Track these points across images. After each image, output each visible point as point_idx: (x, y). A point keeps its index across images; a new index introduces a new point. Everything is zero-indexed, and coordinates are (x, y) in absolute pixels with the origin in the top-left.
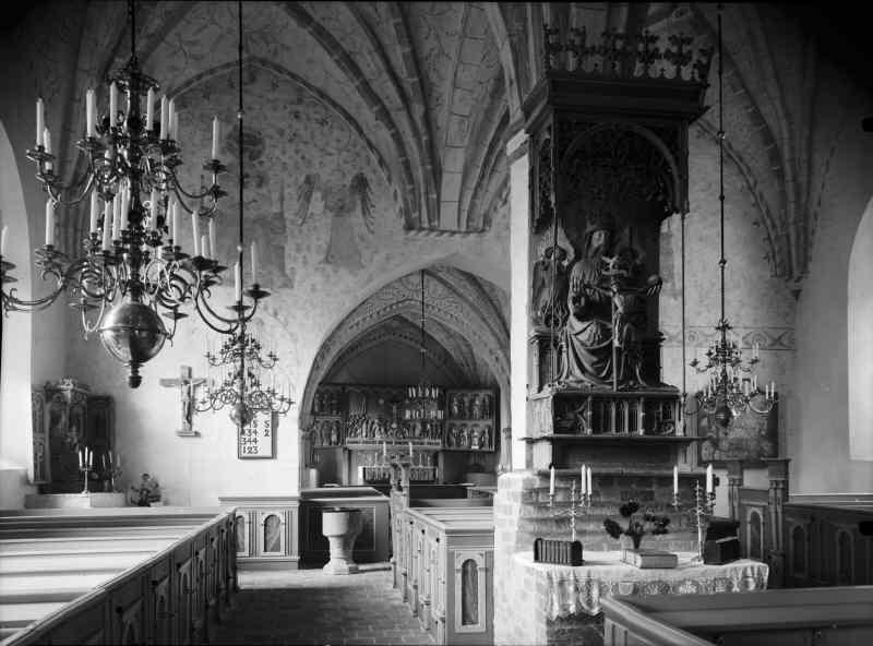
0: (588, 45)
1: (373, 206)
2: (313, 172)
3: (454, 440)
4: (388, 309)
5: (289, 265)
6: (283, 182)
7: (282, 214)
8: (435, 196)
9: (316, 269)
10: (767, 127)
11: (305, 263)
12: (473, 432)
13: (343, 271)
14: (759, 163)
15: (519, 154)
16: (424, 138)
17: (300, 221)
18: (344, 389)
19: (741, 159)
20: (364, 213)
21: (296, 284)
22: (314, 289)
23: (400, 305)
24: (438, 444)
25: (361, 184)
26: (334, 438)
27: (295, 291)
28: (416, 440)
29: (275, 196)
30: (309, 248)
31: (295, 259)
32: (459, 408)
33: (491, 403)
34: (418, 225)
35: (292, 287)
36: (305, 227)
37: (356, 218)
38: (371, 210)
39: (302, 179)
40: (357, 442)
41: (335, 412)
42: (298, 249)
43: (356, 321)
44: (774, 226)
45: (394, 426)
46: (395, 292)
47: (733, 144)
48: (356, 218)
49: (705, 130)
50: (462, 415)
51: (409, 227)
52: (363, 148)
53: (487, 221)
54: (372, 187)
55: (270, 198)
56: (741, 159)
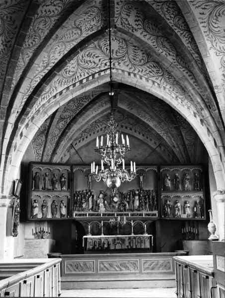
4: (91, 78)
12: (185, 203)
18: (72, 169)
23: (102, 73)
24: (155, 215)
26: (64, 211)
28: (135, 212)
43: (59, 90)
45: (116, 199)
46: (97, 60)
50: (176, 189)
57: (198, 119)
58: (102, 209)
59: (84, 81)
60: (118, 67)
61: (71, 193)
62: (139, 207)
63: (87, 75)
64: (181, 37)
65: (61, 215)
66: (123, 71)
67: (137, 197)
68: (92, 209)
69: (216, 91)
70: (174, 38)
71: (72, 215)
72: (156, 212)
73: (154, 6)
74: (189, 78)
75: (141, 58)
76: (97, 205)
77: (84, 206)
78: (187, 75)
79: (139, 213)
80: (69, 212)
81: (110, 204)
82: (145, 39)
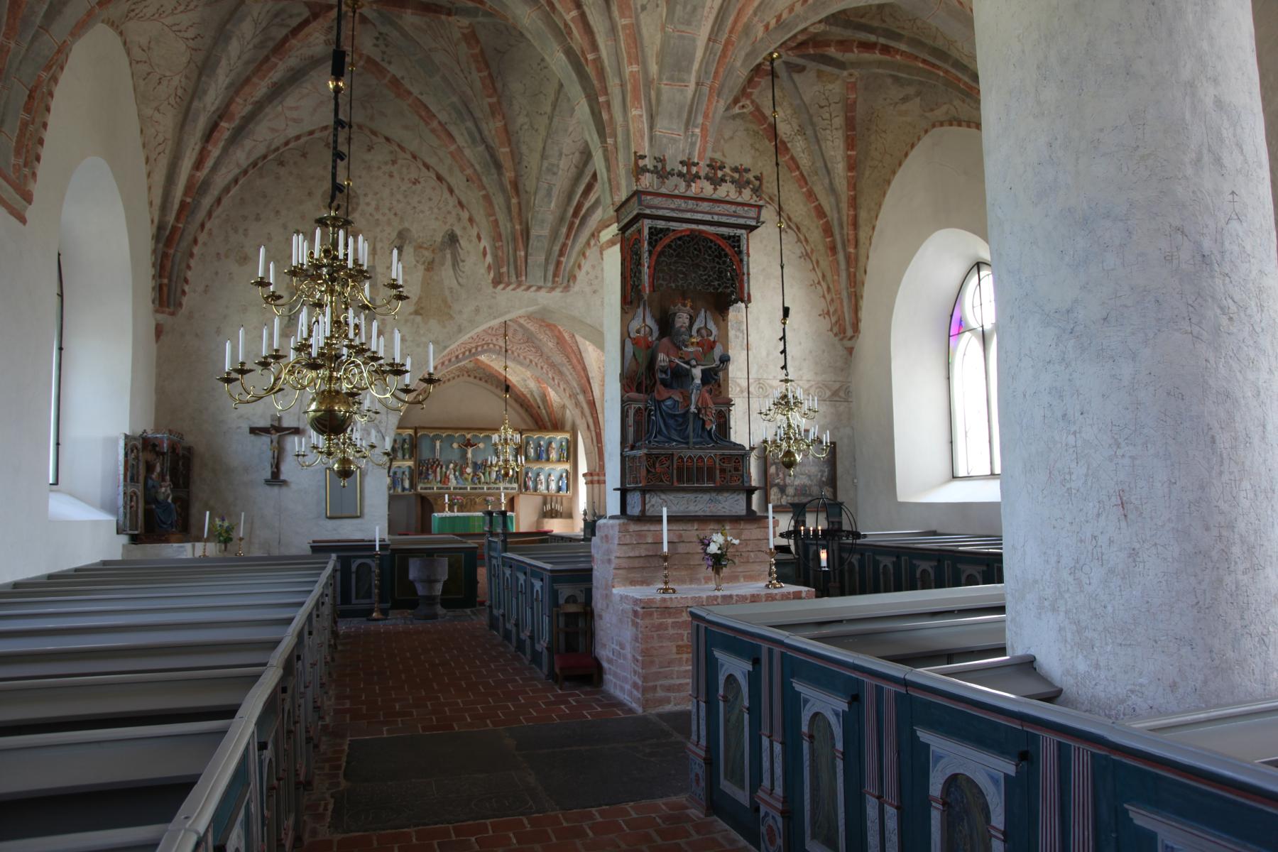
0: (668, 169)
2: (406, 225)
3: (530, 484)
8: (523, 253)
9: (406, 321)
13: (433, 323)
14: (815, 235)
15: (612, 243)
16: (514, 201)
18: (416, 433)
19: (798, 229)
20: (454, 265)
25: (452, 239)
26: (407, 484)
32: (536, 450)
33: (568, 448)
34: (506, 279)
39: (394, 235)
44: (829, 289)
45: (469, 470)
48: (446, 272)
50: (538, 458)
51: (496, 282)
53: (572, 277)
56: (798, 229)
65: (404, 489)
72: (516, 485)
76: (446, 477)
80: (413, 486)
81: (462, 473)
82: (529, 326)
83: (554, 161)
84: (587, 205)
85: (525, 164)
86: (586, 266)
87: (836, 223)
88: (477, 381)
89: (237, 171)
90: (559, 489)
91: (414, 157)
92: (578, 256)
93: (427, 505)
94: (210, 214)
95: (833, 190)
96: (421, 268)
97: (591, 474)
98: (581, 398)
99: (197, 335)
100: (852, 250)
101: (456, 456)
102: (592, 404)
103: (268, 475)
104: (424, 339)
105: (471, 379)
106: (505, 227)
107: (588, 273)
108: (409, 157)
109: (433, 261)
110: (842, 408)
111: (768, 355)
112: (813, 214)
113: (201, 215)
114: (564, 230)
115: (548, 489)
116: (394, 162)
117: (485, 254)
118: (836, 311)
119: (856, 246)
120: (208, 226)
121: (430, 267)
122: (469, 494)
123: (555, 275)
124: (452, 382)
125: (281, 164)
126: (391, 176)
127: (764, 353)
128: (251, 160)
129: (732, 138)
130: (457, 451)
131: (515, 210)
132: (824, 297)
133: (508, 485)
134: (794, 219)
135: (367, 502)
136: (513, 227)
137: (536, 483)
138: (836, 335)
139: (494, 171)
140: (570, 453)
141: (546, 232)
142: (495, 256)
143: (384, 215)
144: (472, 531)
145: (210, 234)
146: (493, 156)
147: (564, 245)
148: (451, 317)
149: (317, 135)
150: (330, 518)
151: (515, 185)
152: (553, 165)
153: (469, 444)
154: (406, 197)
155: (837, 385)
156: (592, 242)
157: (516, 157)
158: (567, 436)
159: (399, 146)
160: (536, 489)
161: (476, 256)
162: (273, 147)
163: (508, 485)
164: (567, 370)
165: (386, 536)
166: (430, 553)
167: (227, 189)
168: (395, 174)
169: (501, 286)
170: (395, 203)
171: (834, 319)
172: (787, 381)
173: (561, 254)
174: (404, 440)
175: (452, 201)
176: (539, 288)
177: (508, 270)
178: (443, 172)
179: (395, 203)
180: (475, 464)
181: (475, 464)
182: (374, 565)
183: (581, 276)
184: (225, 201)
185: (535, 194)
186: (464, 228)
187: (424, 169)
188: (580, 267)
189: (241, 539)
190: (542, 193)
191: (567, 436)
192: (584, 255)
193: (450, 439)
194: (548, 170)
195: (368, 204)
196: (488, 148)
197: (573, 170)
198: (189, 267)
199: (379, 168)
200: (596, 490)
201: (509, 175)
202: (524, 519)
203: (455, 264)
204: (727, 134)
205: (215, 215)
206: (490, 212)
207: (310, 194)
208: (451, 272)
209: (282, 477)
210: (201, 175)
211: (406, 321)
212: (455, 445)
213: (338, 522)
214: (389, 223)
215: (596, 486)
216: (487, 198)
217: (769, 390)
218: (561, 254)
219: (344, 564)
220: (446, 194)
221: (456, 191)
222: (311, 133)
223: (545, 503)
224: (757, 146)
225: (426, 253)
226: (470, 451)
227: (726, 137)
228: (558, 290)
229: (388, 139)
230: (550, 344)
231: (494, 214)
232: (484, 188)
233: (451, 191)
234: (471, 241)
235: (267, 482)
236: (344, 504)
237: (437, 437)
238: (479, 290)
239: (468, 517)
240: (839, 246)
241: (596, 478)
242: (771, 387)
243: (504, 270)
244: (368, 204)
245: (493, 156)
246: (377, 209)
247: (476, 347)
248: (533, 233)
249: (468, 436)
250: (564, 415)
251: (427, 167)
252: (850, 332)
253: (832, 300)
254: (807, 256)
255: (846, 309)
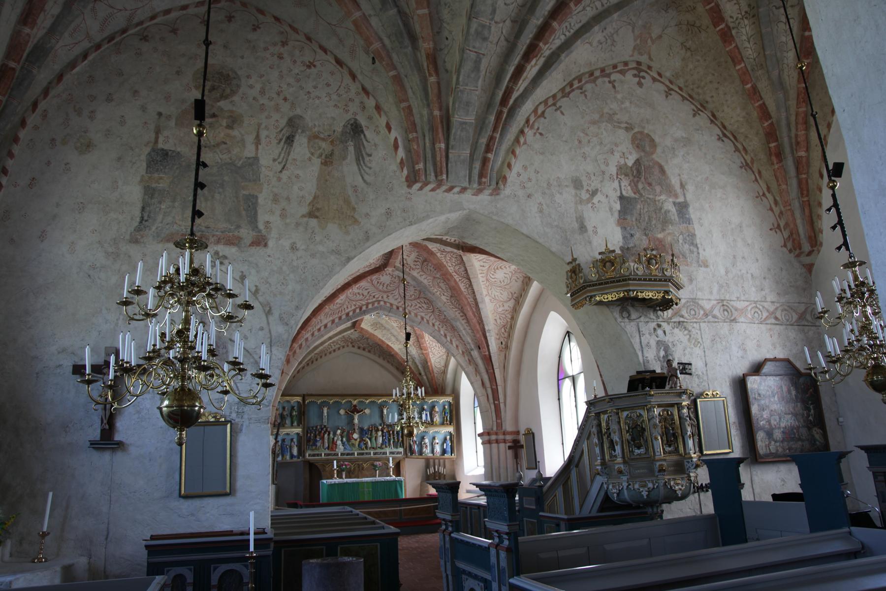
1: (370, 155)
2: (298, 111)
3: (416, 448)
4: (358, 311)
5: (262, 218)
6: (259, 125)
7: (256, 159)
8: (443, 146)
9: (298, 225)
10: (764, 103)
11: (283, 216)
12: (434, 438)
13: (333, 228)
14: (755, 142)
16: (433, 79)
17: (280, 167)
18: (304, 400)
19: (735, 137)
20: (358, 160)
21: (271, 243)
22: (293, 248)
25: (355, 130)
26: (295, 451)
27: (268, 251)
28: (379, 451)
29: (250, 139)
30: (288, 199)
31: (272, 212)
35: (266, 245)
36: (285, 175)
37: (348, 168)
38: (367, 159)
39: (283, 122)
40: (318, 455)
41: (295, 424)
42: (276, 199)
45: (356, 436)
46: (365, 293)
47: (726, 124)
48: (348, 168)
49: (699, 110)
51: (411, 181)
52: (358, 94)
53: (502, 179)
54: (366, 133)
55: (243, 140)
57: (467, 358)
58: (340, 448)
59: (351, 314)
60: (386, 300)
61: (303, 429)
62: (382, 444)
63: (353, 307)
64: (460, 283)
65: (292, 456)
66: (391, 305)
67: (380, 433)
68: (328, 448)
69: (487, 334)
70: (453, 283)
71: (304, 456)
72: (401, 450)
73: (438, 255)
74: (461, 319)
75: (412, 293)
77: (319, 444)
78: (459, 316)
79: (382, 451)
80: (301, 452)
82: (422, 279)
83: (485, 20)
84: (515, 95)
85: (446, 33)
86: (517, 167)
87: (784, 123)
88: (359, 351)
89: (86, 45)
90: (444, 452)
91: (309, 39)
92: (507, 152)
93: (315, 471)
94: (46, 93)
95: (780, 85)
96: (317, 162)
97: (489, 434)
98: (475, 353)
99: (12, 241)
100: (802, 153)
101: (342, 422)
102: (488, 360)
103: (95, 433)
104: (321, 248)
105: (355, 350)
106: (421, 113)
107: (519, 175)
108: (303, 39)
109: (332, 154)
110: (811, 333)
111: (727, 272)
112: (755, 114)
113: (35, 91)
114: (492, 118)
115: (433, 451)
116: (284, 44)
117: (396, 147)
118: (787, 225)
119: (807, 150)
120: (42, 105)
121: (328, 161)
122: (357, 460)
123: (481, 175)
124: (338, 353)
125: (145, 39)
126: (280, 57)
127: (723, 272)
128: (106, 34)
129: (660, 37)
130: (343, 417)
131: (432, 92)
132: (771, 209)
133: (394, 450)
134: (729, 127)
135: (241, 472)
136: (431, 114)
137: (421, 446)
138: (790, 251)
139: (407, 42)
140: (453, 416)
141: (471, 119)
142: (408, 151)
143: (271, 99)
144: (361, 499)
145: (45, 115)
146: (406, 25)
147: (491, 138)
148: (356, 221)
149: (191, 10)
150: (186, 497)
151: (433, 59)
152: (483, 26)
153: (355, 410)
154: (298, 81)
155: (802, 308)
156: (522, 140)
157: (436, 24)
158: (450, 399)
159: (291, 26)
160: (421, 453)
161: (385, 150)
162: (136, 21)
163: (394, 450)
164: (461, 324)
165: (267, 524)
166: (330, 547)
167: (72, 65)
168: (285, 56)
169: (417, 186)
170: (285, 87)
171: (786, 234)
172: (852, 265)
173: (488, 149)
174: (293, 408)
175: (354, 88)
176: (463, 190)
177: (426, 165)
178: (344, 56)
179: (285, 87)
180: (361, 430)
181: (361, 430)
182: (247, 572)
183: (512, 176)
184: (67, 78)
185: (458, 72)
186: (370, 118)
187: (319, 51)
188: (509, 166)
189: (44, 535)
190: (468, 66)
191: (450, 399)
192: (513, 152)
193: (337, 405)
194: (478, 33)
195: (251, 87)
196: (400, 12)
197: (503, 43)
198: (11, 155)
199: (266, 49)
200: (495, 450)
201: (426, 46)
202: (411, 483)
203: (360, 157)
204: (656, 31)
205: (52, 93)
206: (402, 97)
207: (178, 73)
208: (355, 168)
209: (117, 437)
210: (36, 33)
211: (298, 225)
212: (342, 412)
213: (197, 502)
214: (277, 109)
215: (494, 445)
216: (398, 80)
217: (735, 314)
218: (488, 149)
219: (202, 571)
220: (348, 80)
221: (360, 77)
222: (184, 8)
223: (427, 466)
224: (689, 44)
225: (323, 145)
226: (356, 417)
227: (654, 36)
228: (487, 192)
229: (277, 19)
230: (443, 298)
231: (407, 100)
232: (395, 68)
233: (354, 77)
234: (378, 133)
235: (94, 445)
236: (209, 478)
237: (324, 404)
238: (391, 190)
239: (358, 483)
240: (787, 150)
241: (493, 437)
242: (736, 310)
243: (421, 166)
244: (251, 87)
245: (406, 25)
246: (262, 92)
247: (367, 304)
248: (456, 119)
249: (355, 402)
250: (444, 380)
251: (325, 51)
252: (806, 247)
253: (781, 213)
254: (746, 166)
255: (799, 222)
